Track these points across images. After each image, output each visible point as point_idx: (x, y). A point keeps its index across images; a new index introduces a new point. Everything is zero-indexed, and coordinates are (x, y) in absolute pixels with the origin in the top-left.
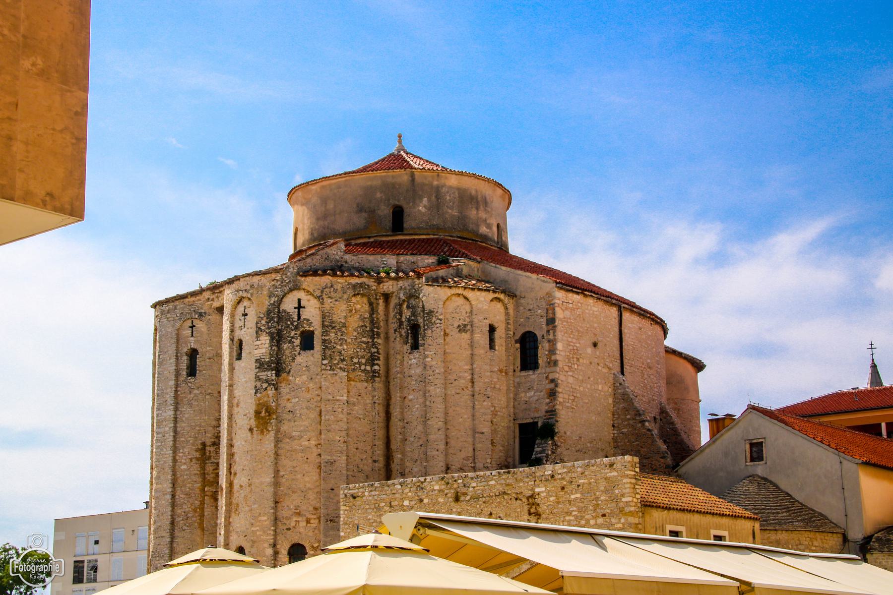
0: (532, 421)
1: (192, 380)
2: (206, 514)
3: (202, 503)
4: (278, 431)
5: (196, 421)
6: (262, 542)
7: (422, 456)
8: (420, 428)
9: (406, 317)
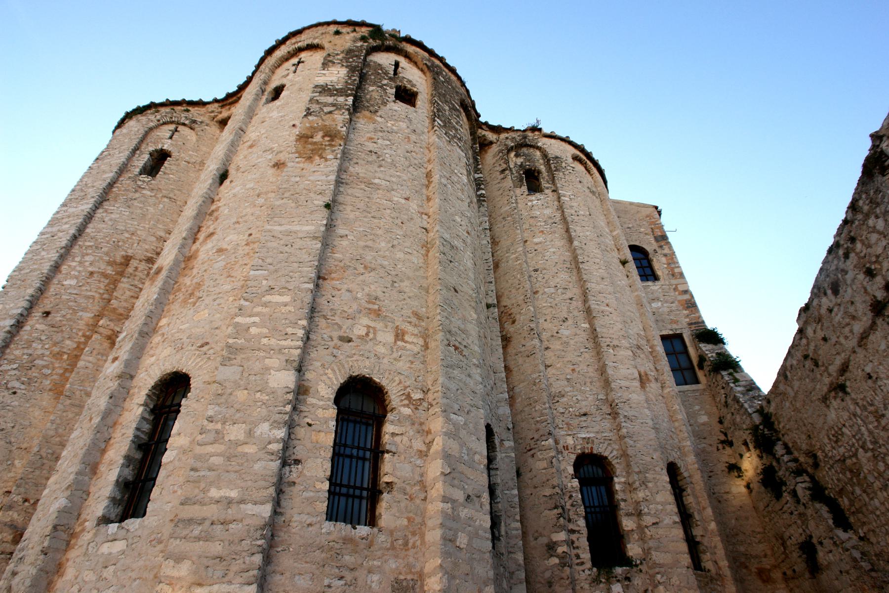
0: (671, 332)
1: (146, 179)
2: (81, 364)
3: (80, 348)
4: (341, 170)
5: (129, 226)
6: (262, 354)
7: (576, 313)
8: (564, 277)
9: (516, 164)
